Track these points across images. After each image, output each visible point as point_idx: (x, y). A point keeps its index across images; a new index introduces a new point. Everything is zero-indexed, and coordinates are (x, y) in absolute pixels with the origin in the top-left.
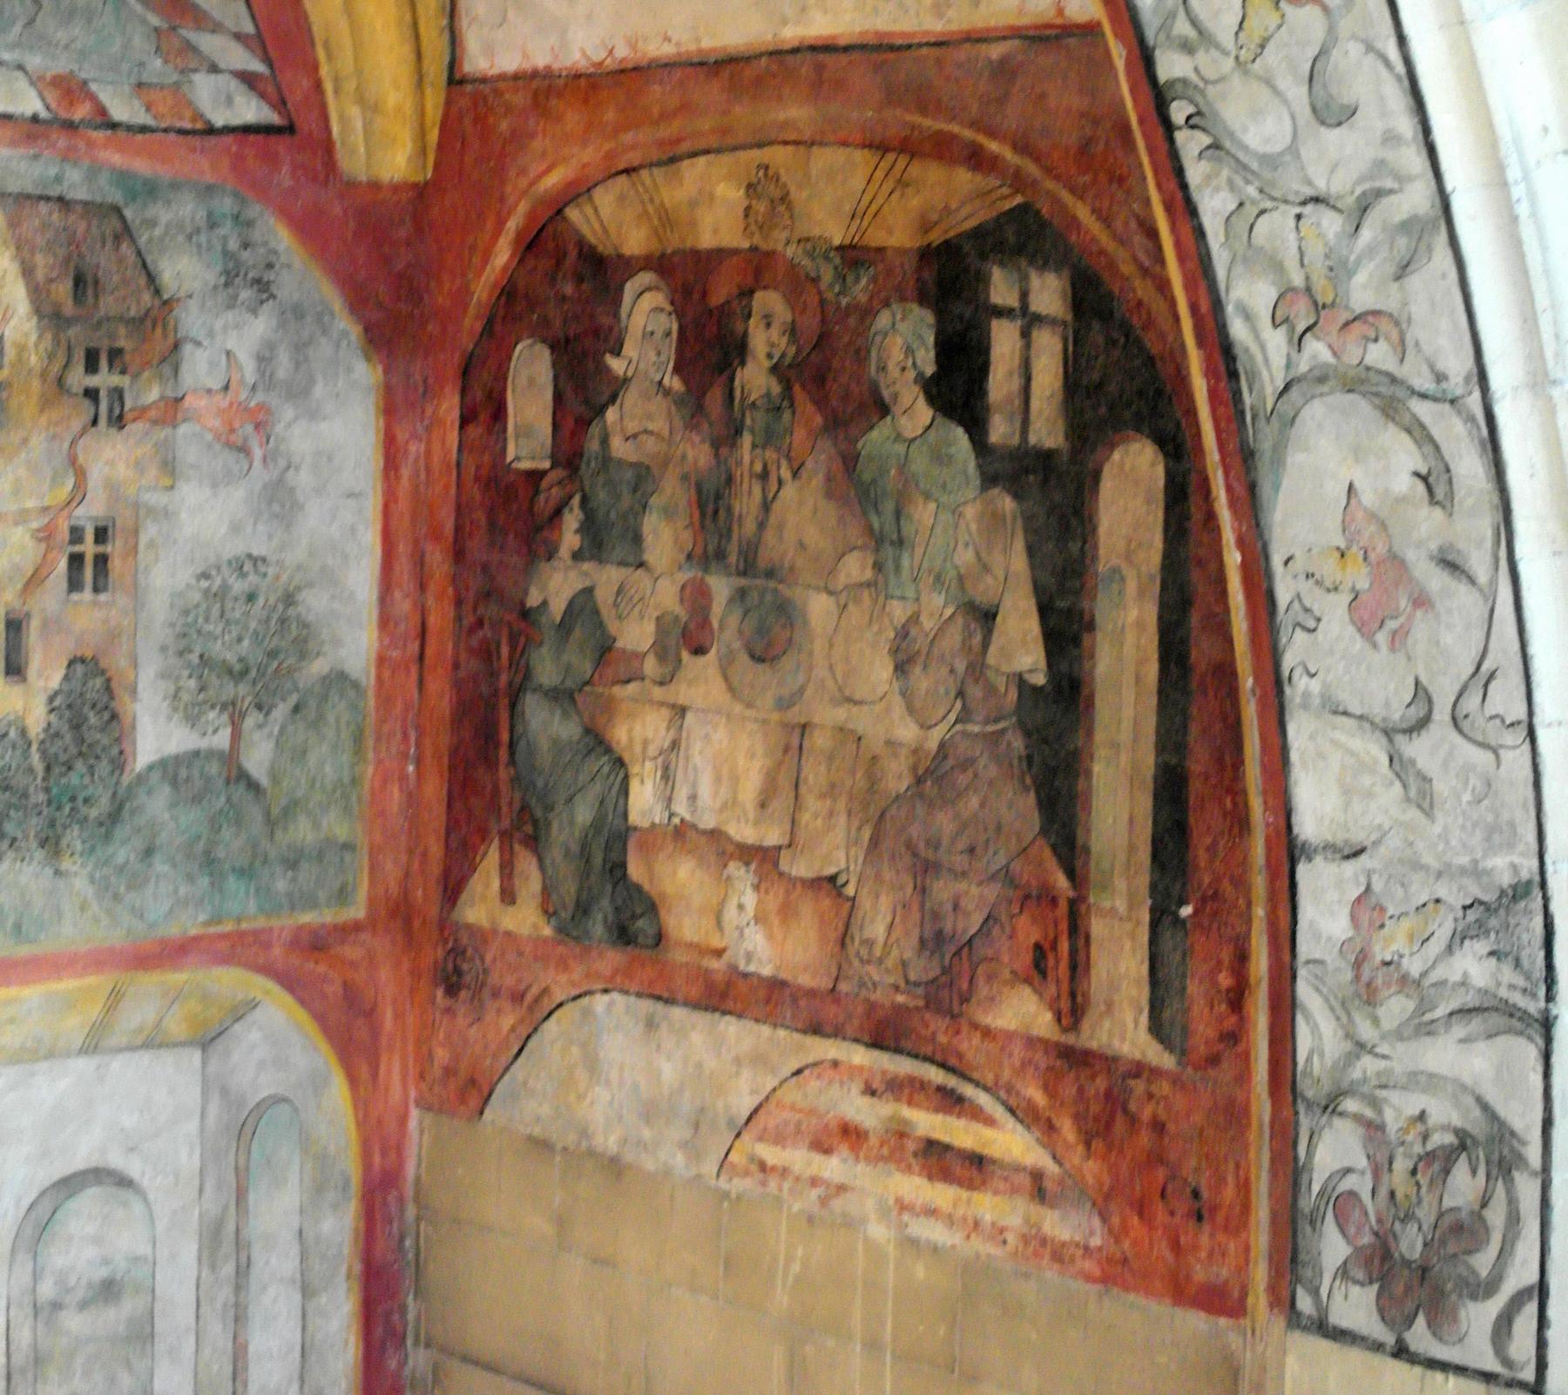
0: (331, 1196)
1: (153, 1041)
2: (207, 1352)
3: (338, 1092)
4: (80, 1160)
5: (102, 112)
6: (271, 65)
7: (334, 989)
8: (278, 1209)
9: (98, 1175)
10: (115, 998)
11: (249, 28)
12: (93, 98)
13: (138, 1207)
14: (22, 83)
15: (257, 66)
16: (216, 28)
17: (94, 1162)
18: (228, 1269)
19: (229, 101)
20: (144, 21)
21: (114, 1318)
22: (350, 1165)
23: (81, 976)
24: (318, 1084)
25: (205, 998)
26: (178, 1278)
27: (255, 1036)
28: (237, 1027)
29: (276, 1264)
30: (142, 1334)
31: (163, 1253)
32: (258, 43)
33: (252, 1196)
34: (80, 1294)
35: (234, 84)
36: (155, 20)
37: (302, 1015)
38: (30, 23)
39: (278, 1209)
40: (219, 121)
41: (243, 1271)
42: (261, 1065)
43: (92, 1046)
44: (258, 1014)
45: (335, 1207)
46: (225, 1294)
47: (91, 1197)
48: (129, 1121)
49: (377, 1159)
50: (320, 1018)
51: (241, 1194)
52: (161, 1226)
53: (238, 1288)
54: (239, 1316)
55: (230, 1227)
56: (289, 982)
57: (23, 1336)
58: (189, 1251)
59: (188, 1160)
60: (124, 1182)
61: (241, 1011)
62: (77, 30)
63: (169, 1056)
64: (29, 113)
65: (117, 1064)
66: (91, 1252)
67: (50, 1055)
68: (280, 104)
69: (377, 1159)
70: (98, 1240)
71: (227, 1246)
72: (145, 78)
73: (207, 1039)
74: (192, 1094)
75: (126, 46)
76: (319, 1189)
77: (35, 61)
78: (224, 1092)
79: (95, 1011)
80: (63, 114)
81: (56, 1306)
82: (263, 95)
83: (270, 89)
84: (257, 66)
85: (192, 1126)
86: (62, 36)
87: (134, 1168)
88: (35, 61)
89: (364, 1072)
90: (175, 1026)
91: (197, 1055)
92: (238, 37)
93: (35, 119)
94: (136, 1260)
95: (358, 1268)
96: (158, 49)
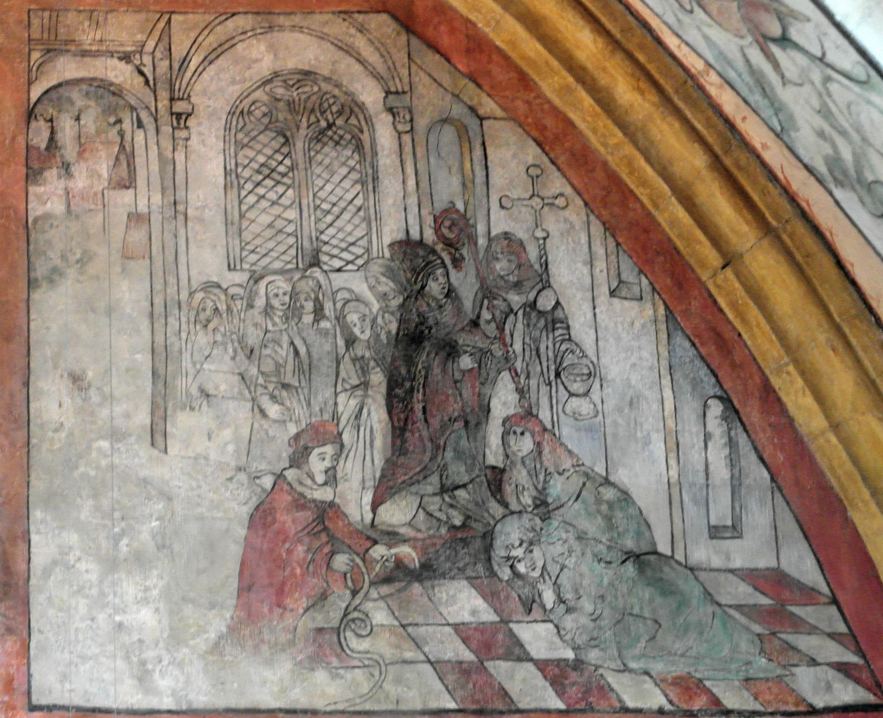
5: (717, 702)
6: (864, 657)
11: (842, 628)
12: (708, 691)
14: (649, 685)
15: (854, 659)
16: (813, 630)
19: (829, 687)
20: (747, 629)
32: (851, 640)
35: (831, 673)
36: (757, 628)
38: (653, 638)
40: (819, 703)
62: (691, 640)
64: (655, 707)
68: (876, 687)
72: (752, 673)
75: (735, 649)
77: (658, 667)
80: (685, 707)
82: (858, 681)
83: (865, 675)
84: (854, 659)
86: (678, 646)
88: (658, 667)
92: (832, 636)
93: (661, 711)
96: (762, 651)
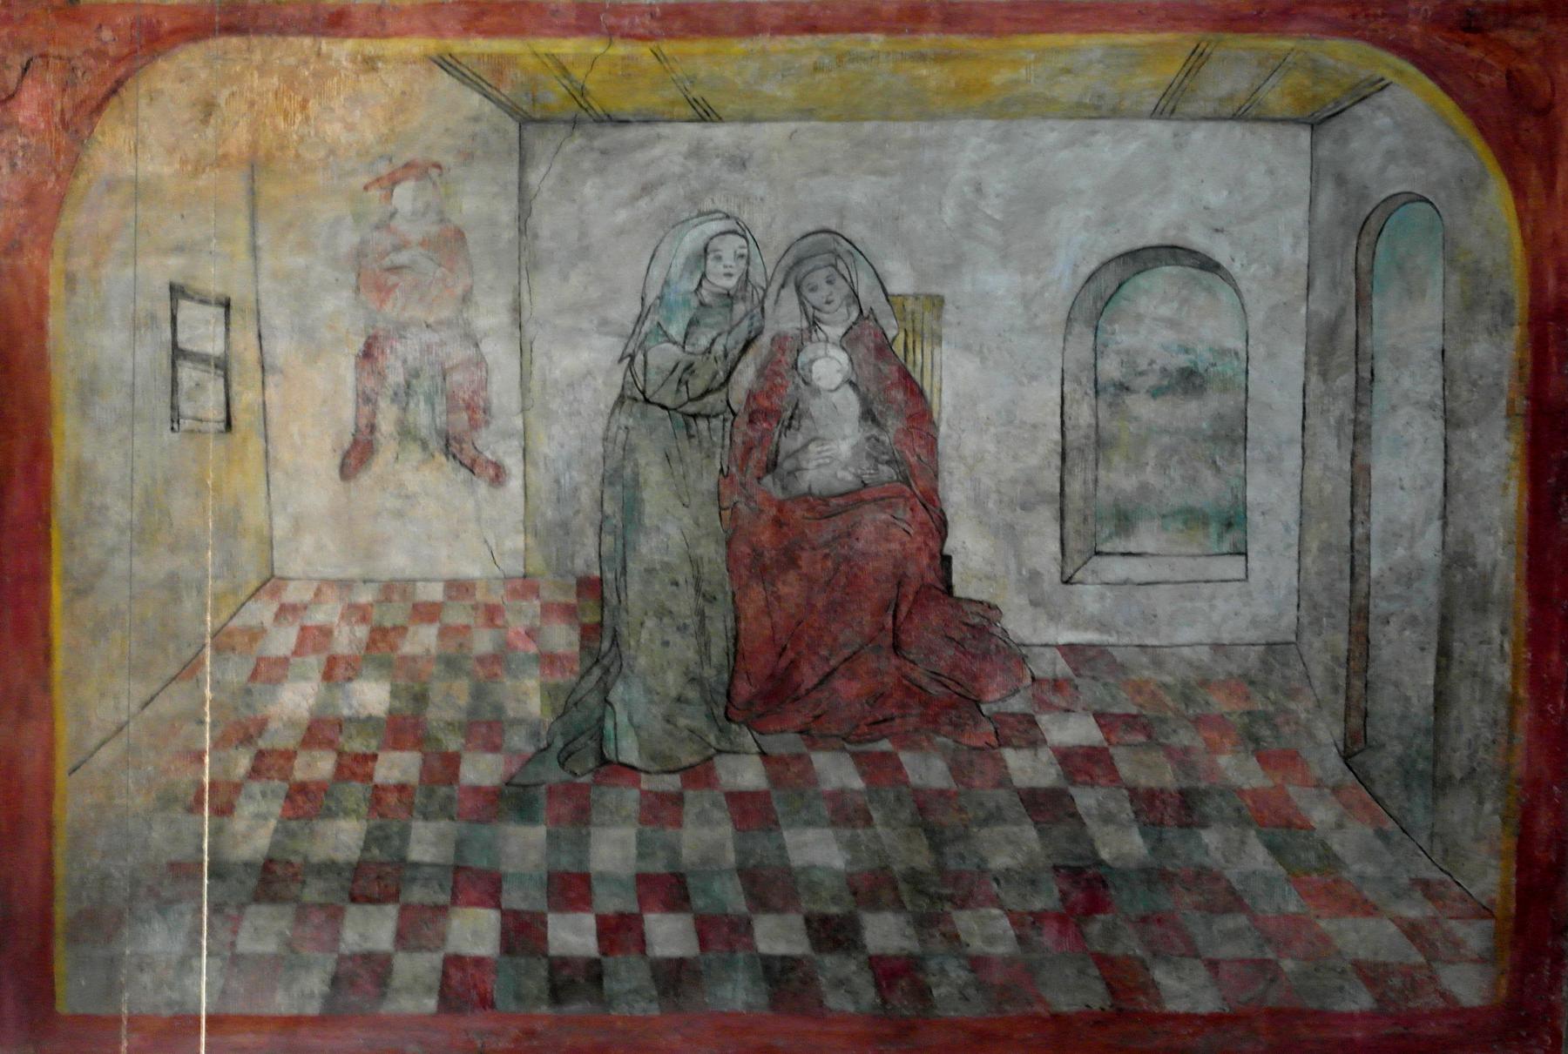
0: (1485, 317)
1: (1246, 113)
2: (1315, 470)
3: (1498, 196)
4: (1155, 227)
7: (1494, 79)
8: (1411, 323)
9: (1174, 253)
10: (1197, 60)
13: (1225, 294)
17: (1171, 237)
18: (1346, 381)
21: (1195, 412)
22: (1516, 284)
23: (1152, 31)
24: (1469, 186)
25: (1316, 70)
26: (1279, 382)
27: (1383, 121)
28: (1360, 110)
29: (1409, 385)
30: (1233, 435)
31: (1258, 351)
33: (1376, 304)
34: (1152, 380)
37: (1448, 105)
39: (1411, 323)
41: (1364, 387)
42: (1391, 156)
43: (1163, 112)
44: (1385, 98)
45: (1492, 330)
46: (1341, 407)
47: (1160, 282)
48: (1215, 198)
49: (1551, 283)
50: (1473, 112)
51: (1362, 301)
52: (1257, 317)
53: (1358, 404)
54: (1360, 435)
55: (1348, 332)
56: (1430, 65)
57: (1082, 414)
58: (1293, 353)
59: (1294, 254)
60: (1209, 265)
61: (1366, 91)
63: (1266, 132)
65: (1200, 134)
66: (1167, 335)
67: (1115, 113)
69: (1551, 283)
70: (1172, 323)
71: (1344, 354)
73: (1318, 120)
74: (1299, 181)
76: (1471, 306)
78: (1340, 180)
79: (1171, 71)
81: (1123, 388)
85: (1299, 214)
87: (1220, 251)
89: (1534, 178)
90: (1275, 98)
91: (1305, 136)
94: (1223, 352)
95: (1522, 404)
